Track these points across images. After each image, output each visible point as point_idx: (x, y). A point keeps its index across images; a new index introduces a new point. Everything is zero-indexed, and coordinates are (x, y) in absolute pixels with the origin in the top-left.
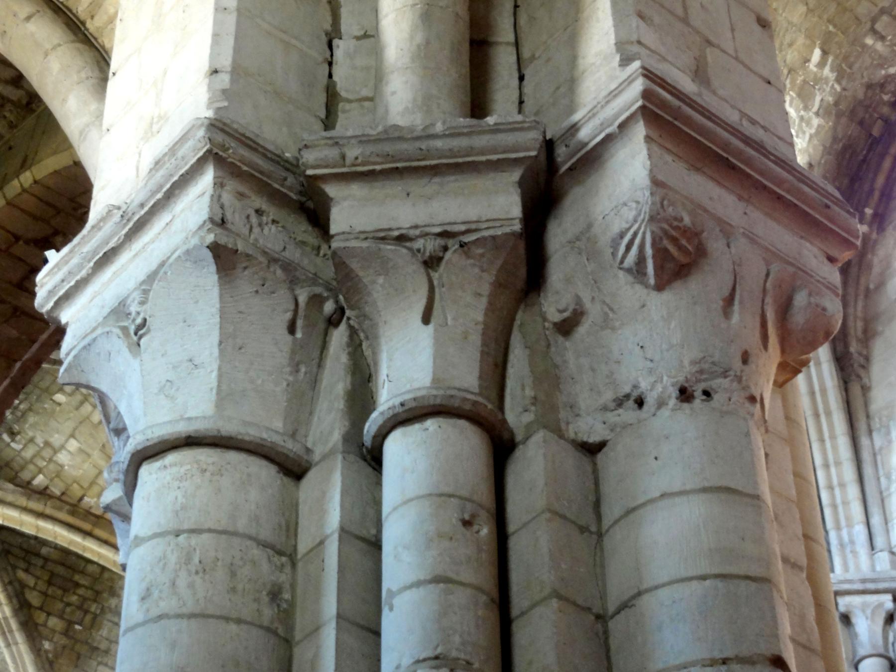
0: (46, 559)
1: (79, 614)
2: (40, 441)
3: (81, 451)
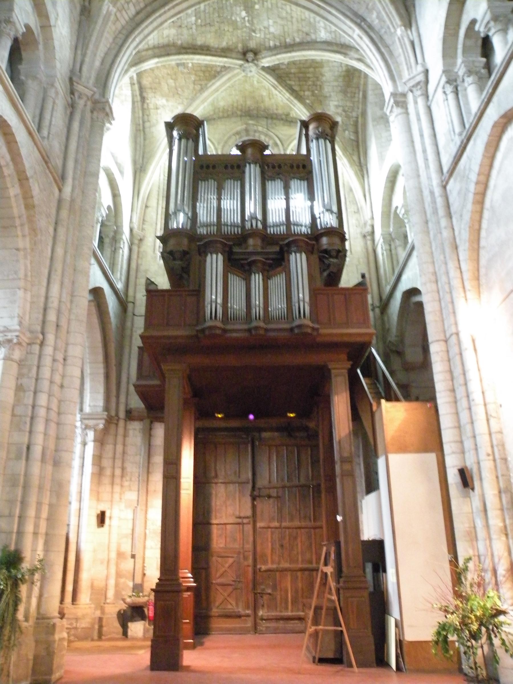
0: (294, 74)
1: (314, 87)
2: (262, 28)
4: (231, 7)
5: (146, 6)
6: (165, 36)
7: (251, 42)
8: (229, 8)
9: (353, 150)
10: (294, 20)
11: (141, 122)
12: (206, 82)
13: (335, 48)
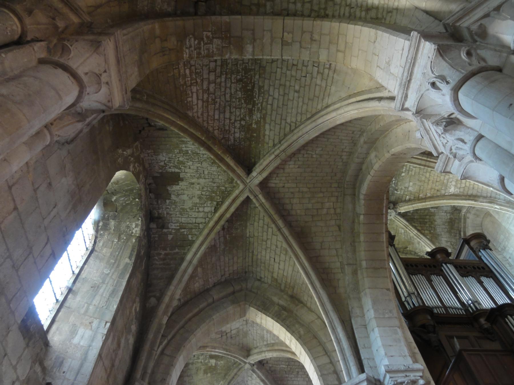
1: (430, 228)
13: (464, 197)
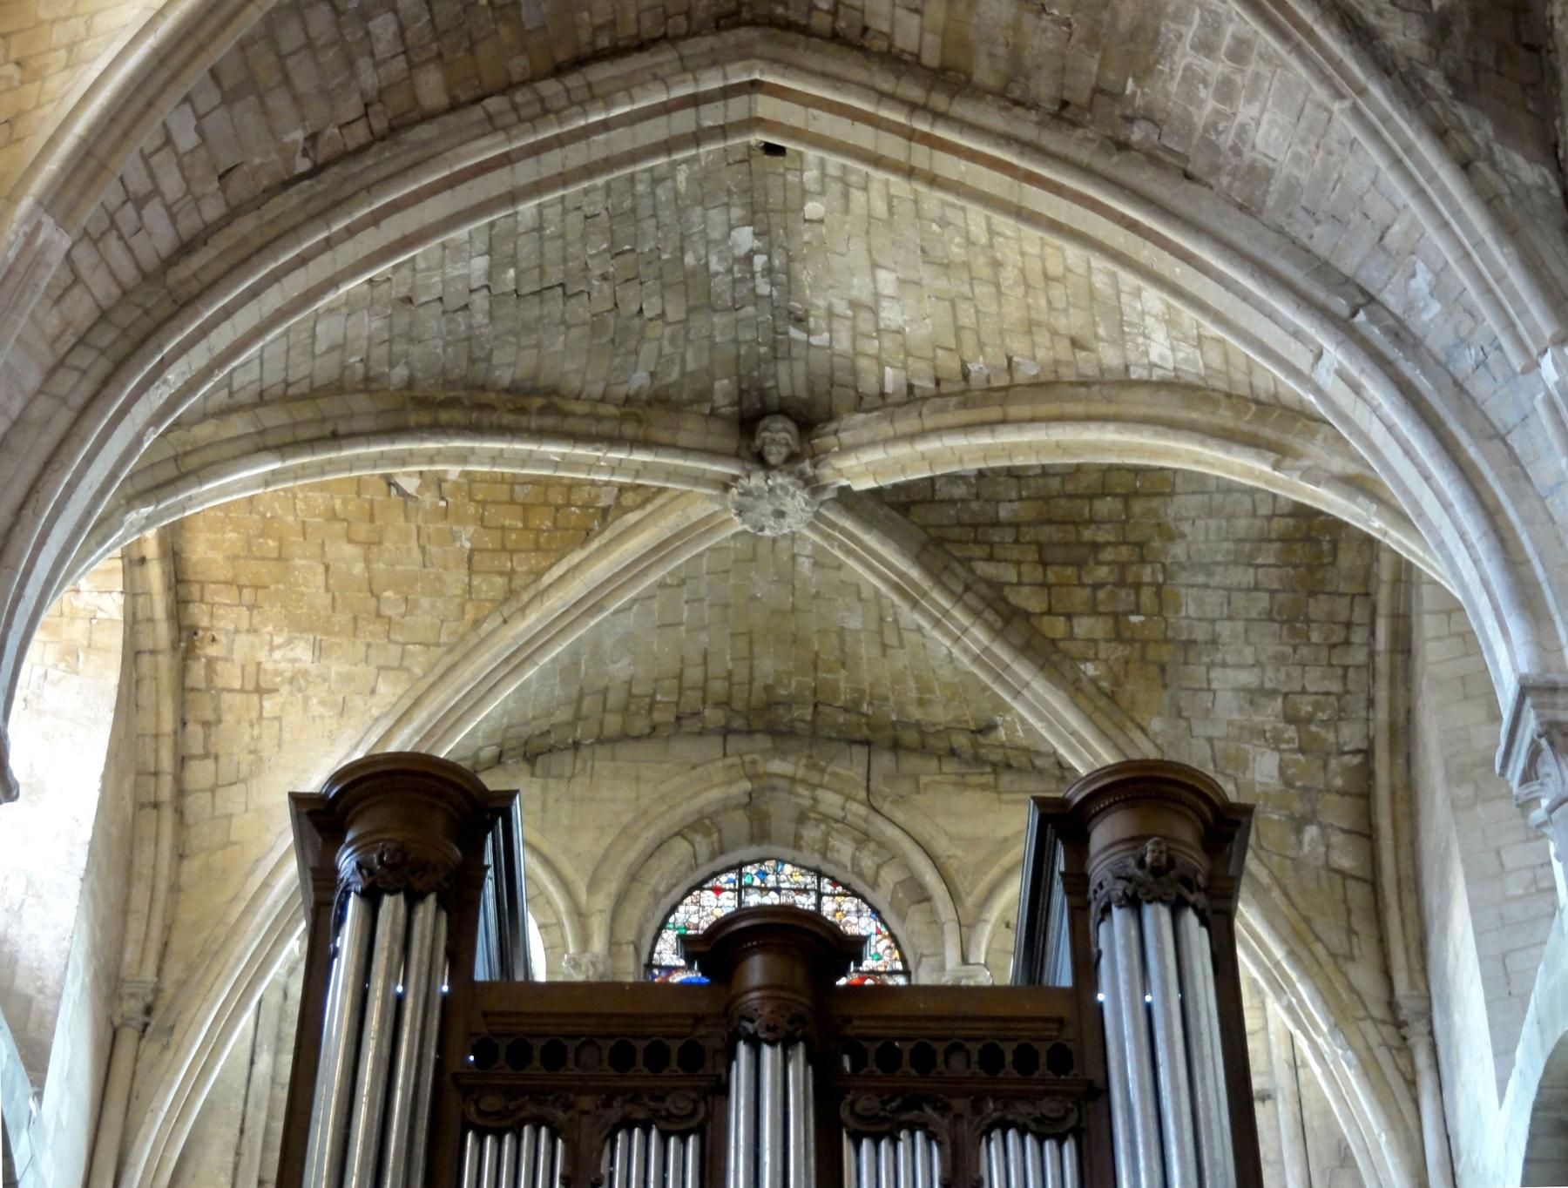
0: (1016, 525)
1: (1125, 597)
2: (841, 307)
3: (902, 282)
4: (680, 211)
5: (233, 214)
6: (321, 347)
7: (783, 369)
8: (666, 215)
9: (1351, 931)
10: (1009, 275)
11: (167, 761)
12: (534, 560)
